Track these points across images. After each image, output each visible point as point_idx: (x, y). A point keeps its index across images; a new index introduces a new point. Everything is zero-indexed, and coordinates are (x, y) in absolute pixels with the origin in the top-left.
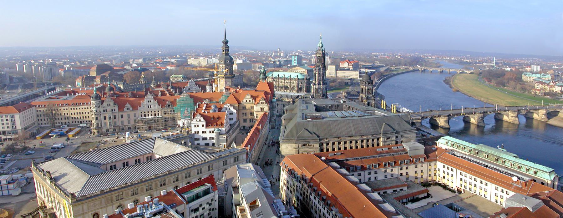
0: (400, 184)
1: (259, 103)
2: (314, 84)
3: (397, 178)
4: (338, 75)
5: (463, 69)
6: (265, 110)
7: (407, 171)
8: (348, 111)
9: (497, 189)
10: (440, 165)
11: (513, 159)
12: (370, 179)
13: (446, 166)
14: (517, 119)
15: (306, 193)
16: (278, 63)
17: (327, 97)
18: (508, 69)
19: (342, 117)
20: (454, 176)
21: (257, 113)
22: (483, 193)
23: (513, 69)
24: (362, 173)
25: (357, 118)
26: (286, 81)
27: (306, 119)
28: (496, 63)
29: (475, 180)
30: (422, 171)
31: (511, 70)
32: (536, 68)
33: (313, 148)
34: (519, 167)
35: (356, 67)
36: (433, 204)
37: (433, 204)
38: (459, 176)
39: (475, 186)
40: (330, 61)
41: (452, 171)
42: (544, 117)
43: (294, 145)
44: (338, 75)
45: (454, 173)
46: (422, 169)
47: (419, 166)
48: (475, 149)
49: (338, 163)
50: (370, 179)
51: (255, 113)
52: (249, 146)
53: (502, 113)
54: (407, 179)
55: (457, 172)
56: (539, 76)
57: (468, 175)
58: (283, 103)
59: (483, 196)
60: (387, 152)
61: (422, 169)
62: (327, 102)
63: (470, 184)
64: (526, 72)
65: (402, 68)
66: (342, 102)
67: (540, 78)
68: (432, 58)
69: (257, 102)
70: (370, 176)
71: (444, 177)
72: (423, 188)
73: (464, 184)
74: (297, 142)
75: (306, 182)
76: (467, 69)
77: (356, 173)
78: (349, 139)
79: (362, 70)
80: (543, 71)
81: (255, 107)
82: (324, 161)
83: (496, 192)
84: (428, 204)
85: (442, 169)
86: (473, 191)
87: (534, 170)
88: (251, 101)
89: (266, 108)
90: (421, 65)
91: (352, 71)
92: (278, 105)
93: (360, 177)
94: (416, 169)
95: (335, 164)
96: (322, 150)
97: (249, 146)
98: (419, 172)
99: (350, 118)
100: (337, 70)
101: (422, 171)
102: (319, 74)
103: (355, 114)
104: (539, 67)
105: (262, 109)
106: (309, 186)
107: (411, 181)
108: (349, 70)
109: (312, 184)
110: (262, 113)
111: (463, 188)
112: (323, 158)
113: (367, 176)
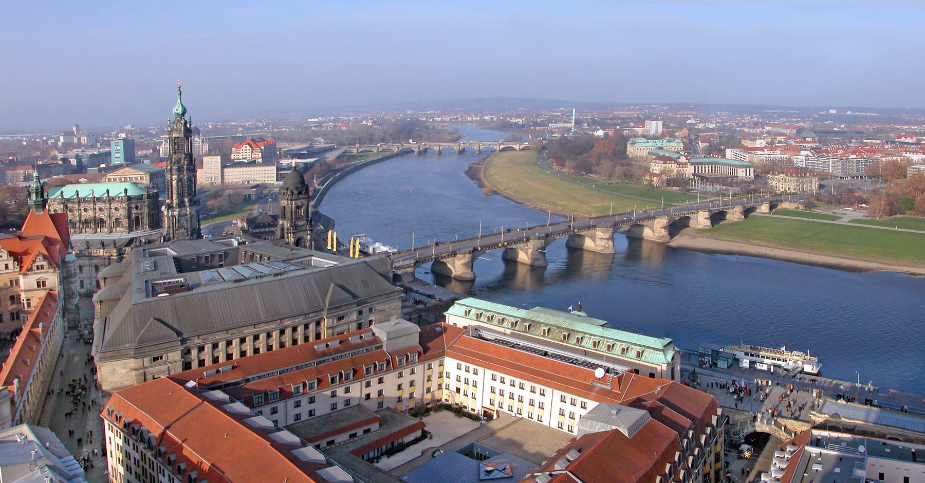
0: (363, 418)
1: (30, 269)
2: (170, 207)
3: (358, 405)
4: (228, 180)
5: (507, 140)
6: (48, 285)
7: (381, 387)
8: (251, 265)
9: (563, 400)
10: (450, 364)
11: (599, 331)
12: (298, 417)
13: (464, 364)
14: (611, 243)
15: (149, 470)
16: (74, 162)
17: (200, 236)
18: (600, 133)
19: (236, 281)
20: (480, 385)
21: (30, 295)
22: (536, 411)
23: (611, 133)
24: (280, 406)
26: (98, 205)
27: (155, 293)
28: (577, 122)
30: (412, 384)
31: (606, 135)
32: (655, 127)
33: (166, 363)
34: (609, 346)
35: (270, 157)
36: (434, 453)
37: (434, 453)
38: (489, 383)
39: (521, 400)
40: (206, 148)
41: (476, 373)
42: (664, 232)
43: (132, 363)
44: (228, 180)
45: (479, 379)
49: (225, 392)
50: (298, 417)
51: (23, 296)
52: (16, 381)
53: (582, 233)
54: (380, 404)
55: (485, 377)
56: (659, 144)
57: (508, 378)
58: (95, 262)
59: (535, 420)
60: (337, 351)
61: (413, 377)
62: (204, 247)
64: (635, 136)
65: (375, 150)
66: (236, 244)
67: (660, 148)
68: (442, 121)
69: (26, 265)
70: (297, 411)
71: (458, 390)
72: (413, 421)
73: (497, 398)
74: (138, 353)
75: (150, 447)
76: (515, 139)
77: (267, 409)
78: (252, 330)
79: (285, 162)
80: (669, 133)
81: (22, 280)
82: (192, 390)
83: (562, 405)
84: (423, 453)
85: (454, 372)
86: (515, 410)
87: (638, 348)
88: (11, 266)
89: (52, 279)
90: (418, 138)
91: (259, 165)
92: (81, 267)
93: (275, 417)
94: (400, 381)
95: (219, 395)
96: (187, 366)
97: (16, 381)
98: (406, 386)
99: (254, 281)
100: (224, 166)
101: (412, 384)
102: (179, 180)
103: (266, 270)
104: (660, 123)
105: (41, 284)
106: (159, 454)
107: (388, 408)
108: (253, 163)
109: (163, 449)
110: (42, 294)
111: (496, 408)
112: (191, 384)
113: (292, 411)
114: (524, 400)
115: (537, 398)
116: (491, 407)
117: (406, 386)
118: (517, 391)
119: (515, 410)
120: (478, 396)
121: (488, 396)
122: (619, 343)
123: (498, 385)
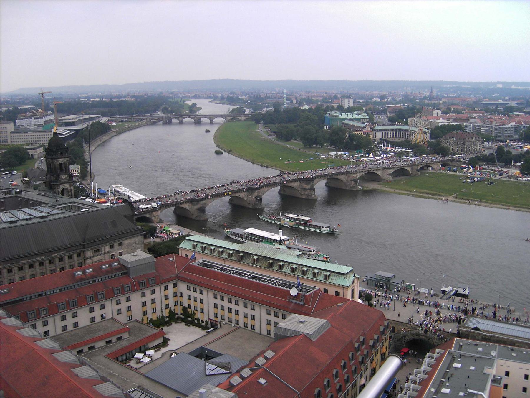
3: (112, 318)
7: (129, 304)
20: (205, 301)
25: (39, 220)
29: (237, 304)
30: (153, 301)
34: (303, 271)
36: (172, 354)
41: (201, 293)
45: (204, 297)
46: (153, 296)
47: (148, 292)
48: (238, 252)
50: (65, 328)
61: (153, 296)
63: (230, 310)
70: (64, 323)
72: (155, 331)
85: (185, 293)
86: (234, 321)
94: (144, 299)
98: (149, 303)
101: (153, 301)
107: (136, 321)
111: (219, 319)
114: (240, 313)
115: (249, 311)
116: (216, 319)
117: (149, 303)
118: (233, 306)
119: (234, 321)
120: (205, 311)
121: (212, 310)
122: (311, 269)
123: (218, 301)
